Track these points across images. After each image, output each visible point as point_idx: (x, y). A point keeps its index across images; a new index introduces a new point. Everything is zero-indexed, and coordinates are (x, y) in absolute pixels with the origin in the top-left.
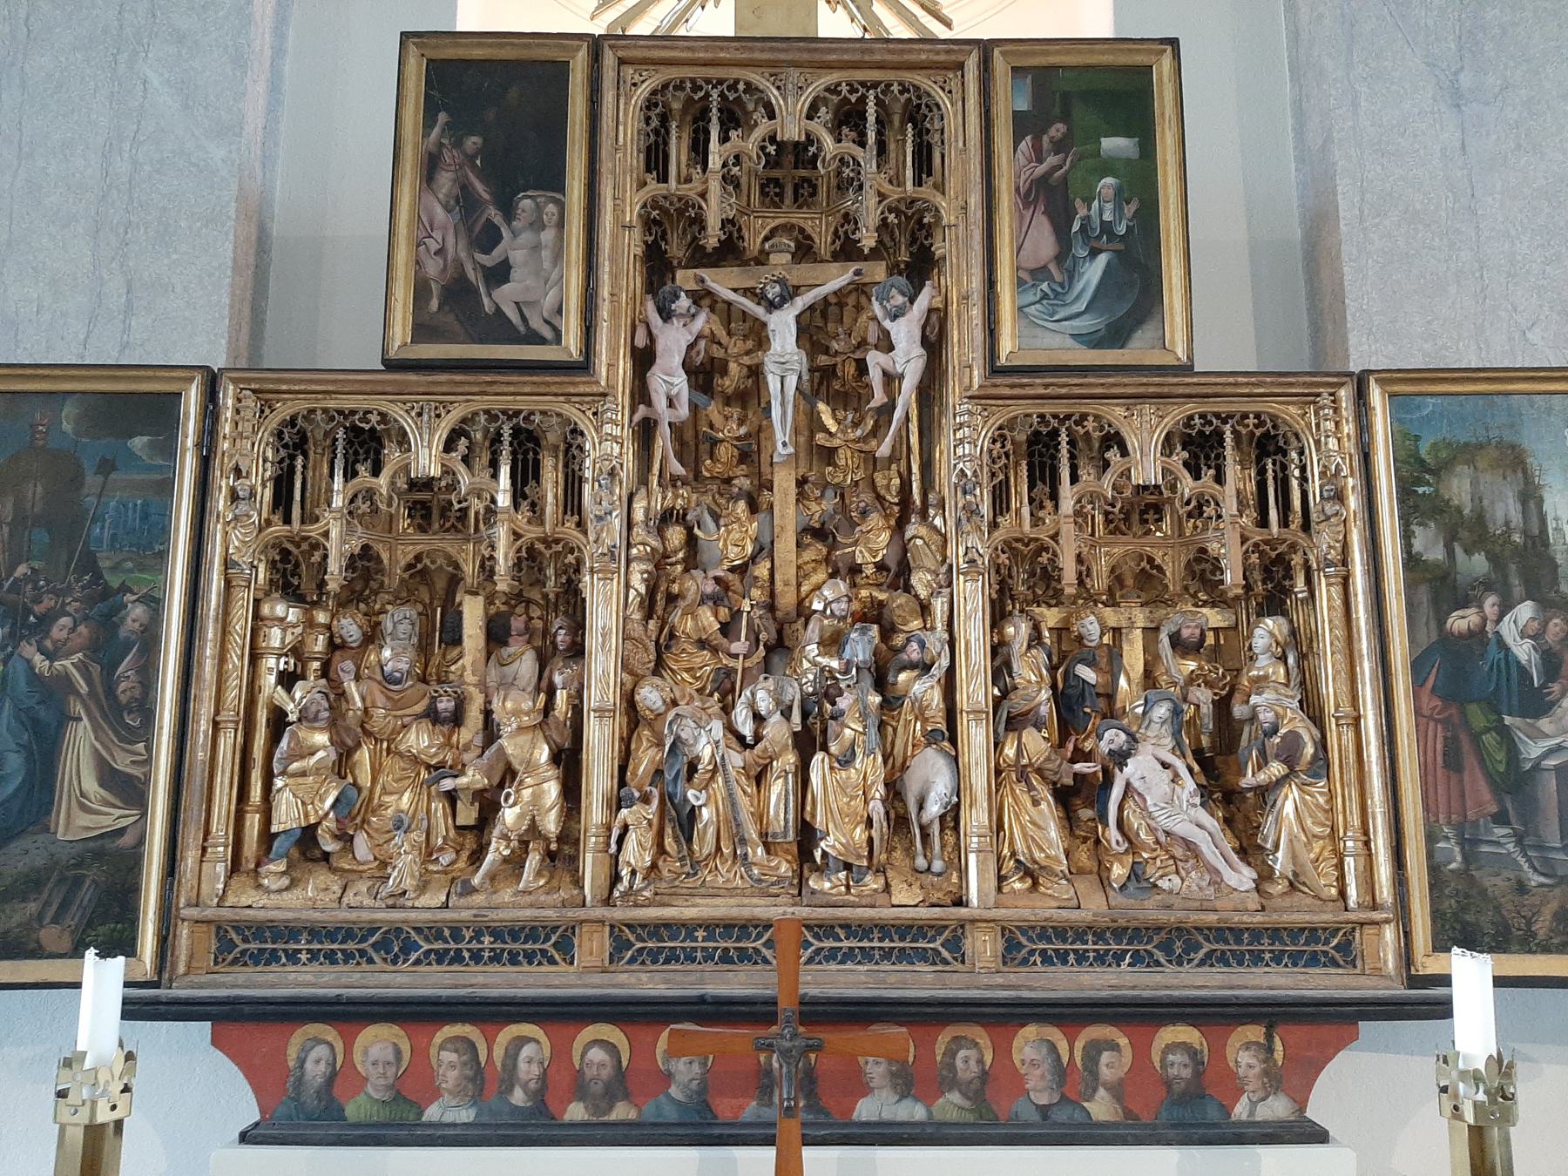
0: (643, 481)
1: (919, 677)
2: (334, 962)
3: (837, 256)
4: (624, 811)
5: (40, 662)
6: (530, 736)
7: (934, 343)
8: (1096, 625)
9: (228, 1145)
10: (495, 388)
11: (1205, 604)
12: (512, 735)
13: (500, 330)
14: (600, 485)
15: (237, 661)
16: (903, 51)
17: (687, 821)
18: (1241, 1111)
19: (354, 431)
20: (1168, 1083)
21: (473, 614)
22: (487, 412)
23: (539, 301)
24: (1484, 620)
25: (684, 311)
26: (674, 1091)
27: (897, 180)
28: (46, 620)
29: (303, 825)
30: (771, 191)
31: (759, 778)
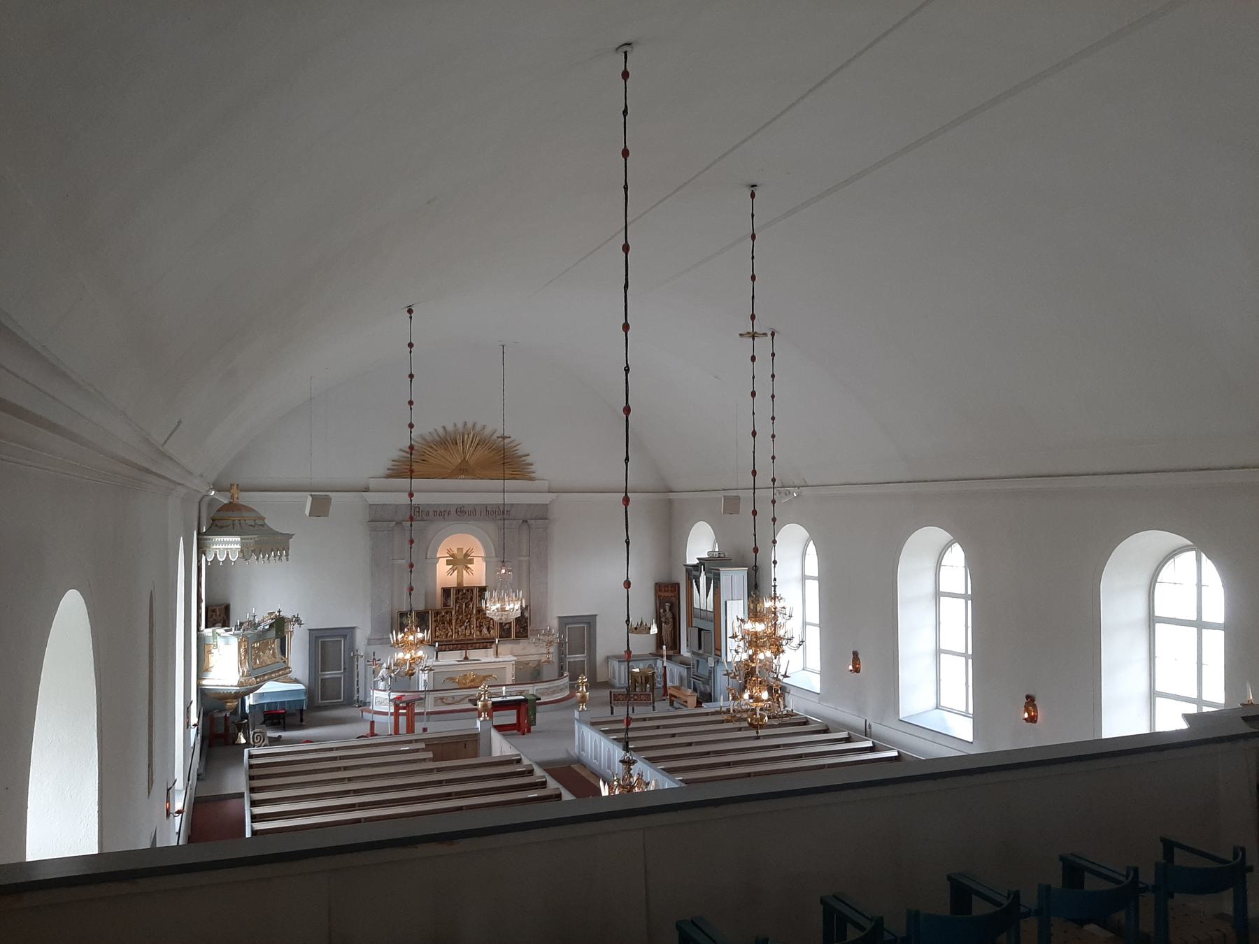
13: (447, 606)
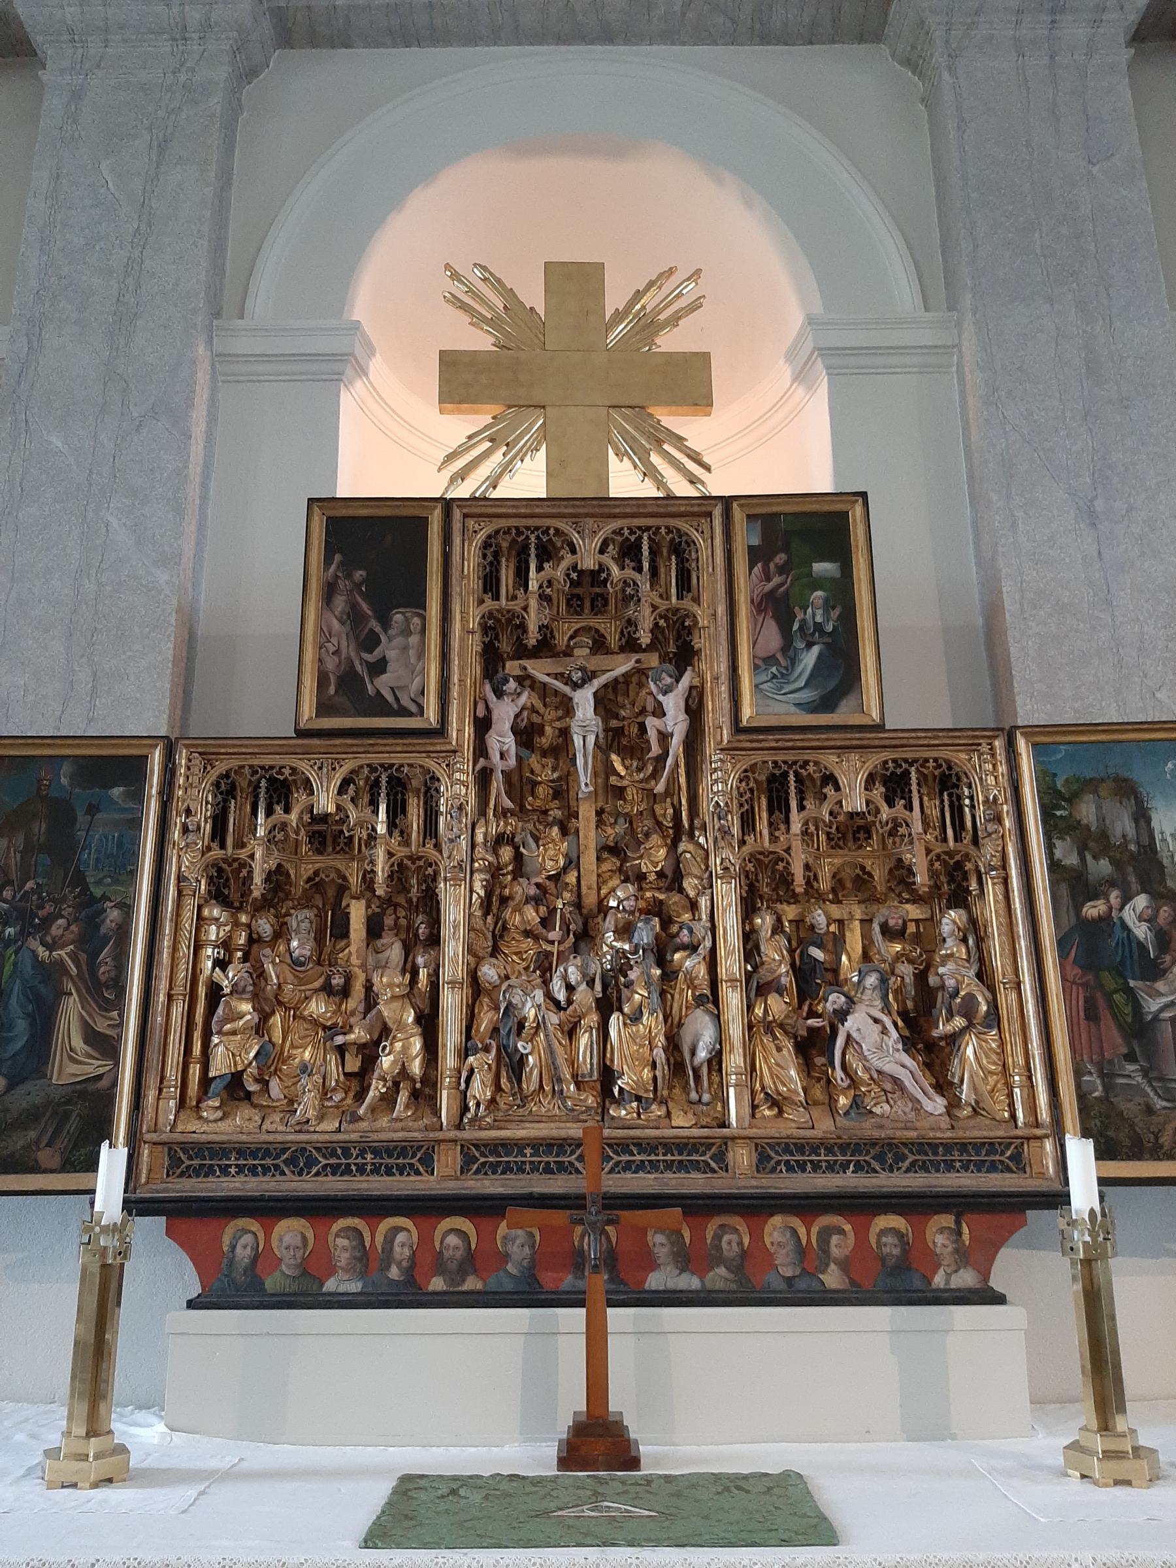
0: (482, 812)
1: (689, 956)
2: (255, 1174)
3: (622, 649)
4: (471, 1059)
5: (42, 953)
6: (400, 1003)
7: (694, 710)
8: (823, 916)
9: (181, 1309)
10: (376, 749)
11: (908, 901)
12: (387, 1002)
13: (380, 707)
14: (451, 817)
15: (185, 949)
16: (667, 505)
17: (517, 1066)
18: (939, 1280)
19: (272, 781)
20: (883, 1259)
21: (357, 913)
22: (369, 765)
23: (407, 687)
24: (1111, 908)
25: (512, 691)
26: (510, 1267)
27: (665, 596)
28: (48, 921)
29: (233, 1071)
30: (575, 603)
31: (571, 1033)
